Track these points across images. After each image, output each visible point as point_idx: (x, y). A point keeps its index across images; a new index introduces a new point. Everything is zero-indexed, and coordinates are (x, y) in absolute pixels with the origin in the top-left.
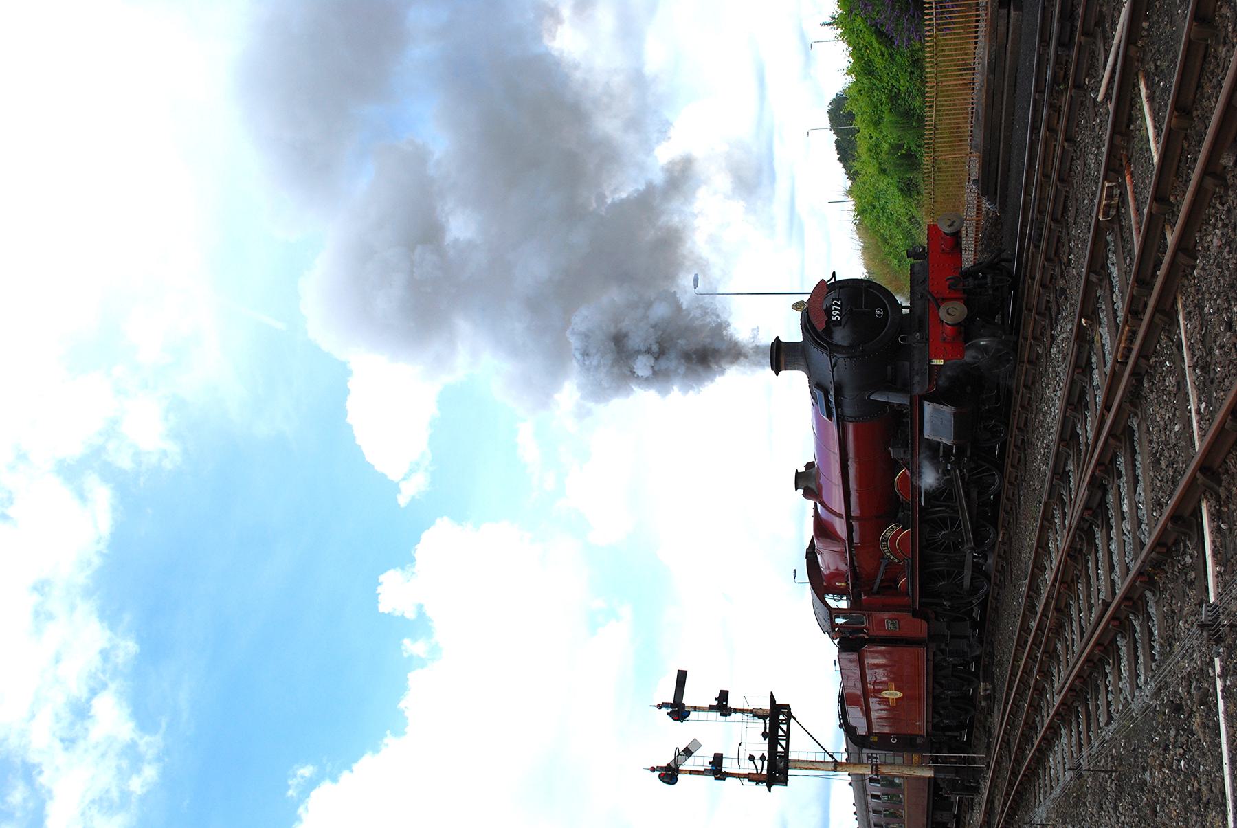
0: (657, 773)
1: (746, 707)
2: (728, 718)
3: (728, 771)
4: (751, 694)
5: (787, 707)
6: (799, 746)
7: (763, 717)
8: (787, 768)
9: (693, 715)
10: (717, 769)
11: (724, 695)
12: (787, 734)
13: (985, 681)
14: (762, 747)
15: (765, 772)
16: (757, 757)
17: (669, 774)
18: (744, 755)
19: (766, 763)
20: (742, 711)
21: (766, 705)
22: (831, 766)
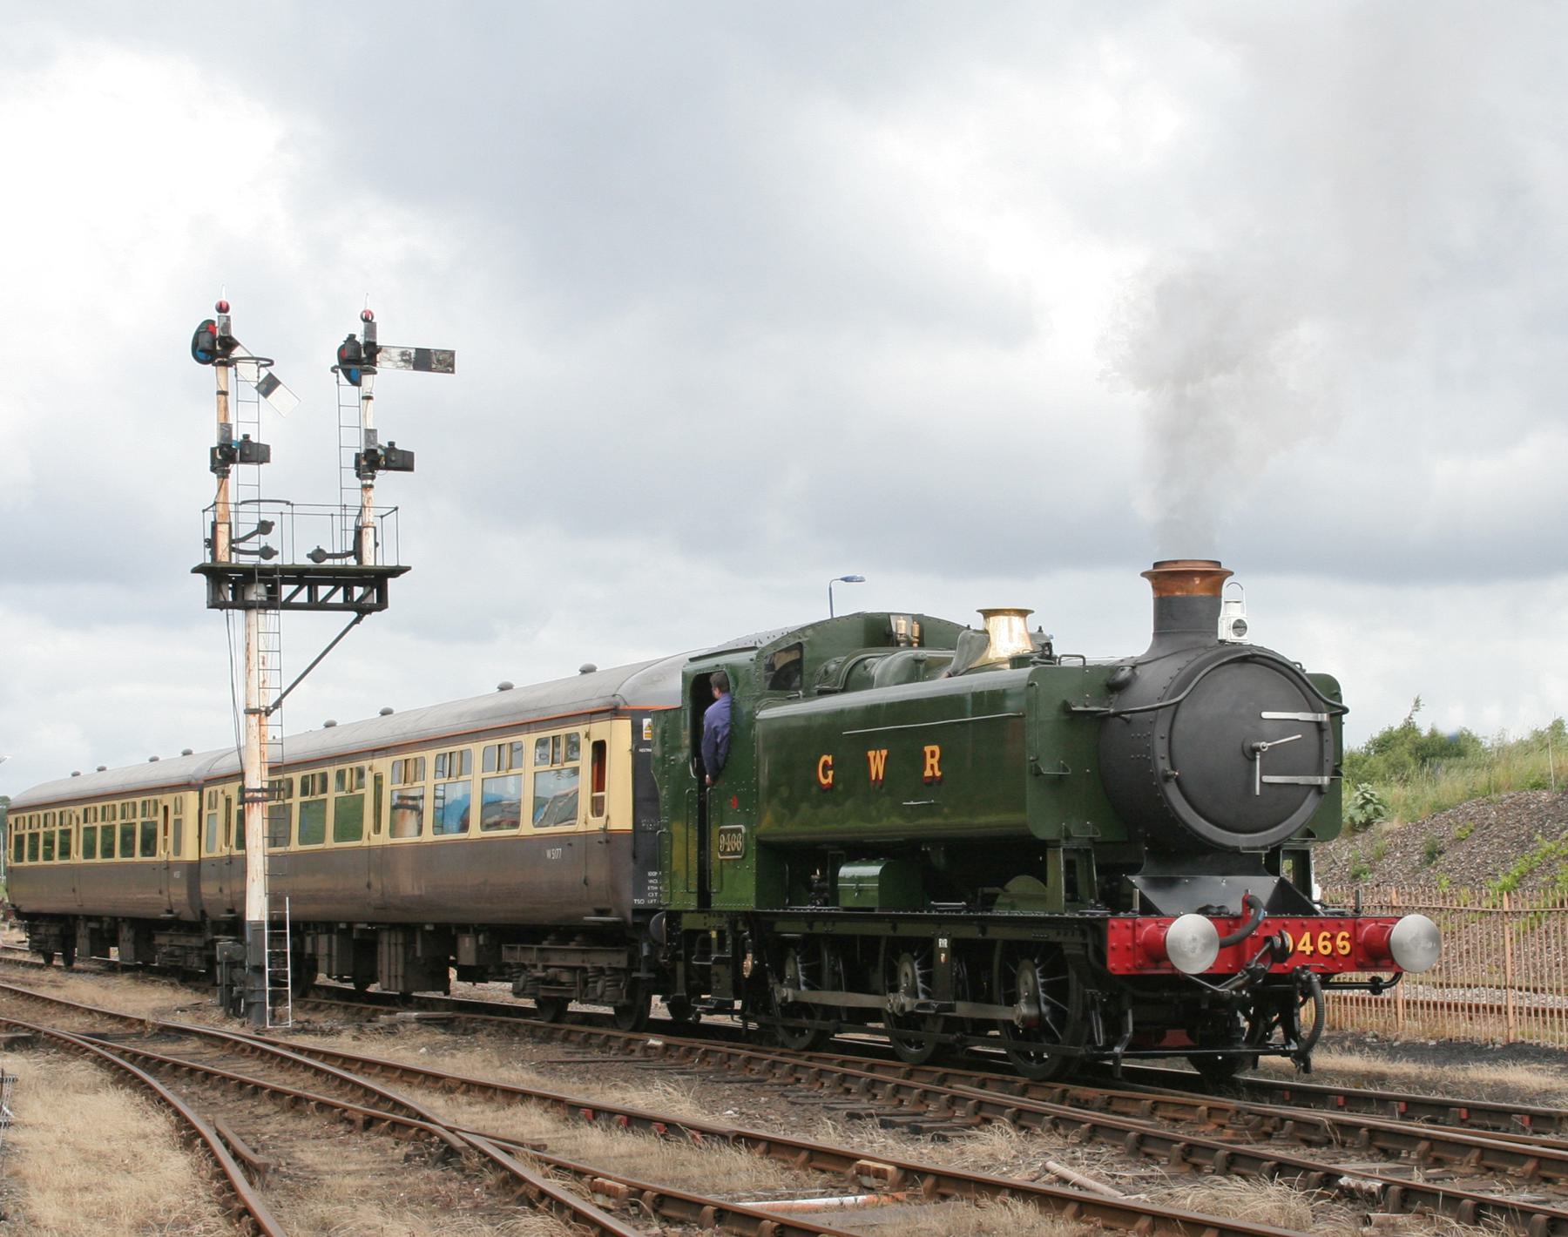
0: (214, 315)
4: (402, 524)
5: (382, 604)
6: (297, 631)
8: (248, 607)
10: (231, 453)
11: (400, 461)
12: (324, 606)
18: (269, 513)
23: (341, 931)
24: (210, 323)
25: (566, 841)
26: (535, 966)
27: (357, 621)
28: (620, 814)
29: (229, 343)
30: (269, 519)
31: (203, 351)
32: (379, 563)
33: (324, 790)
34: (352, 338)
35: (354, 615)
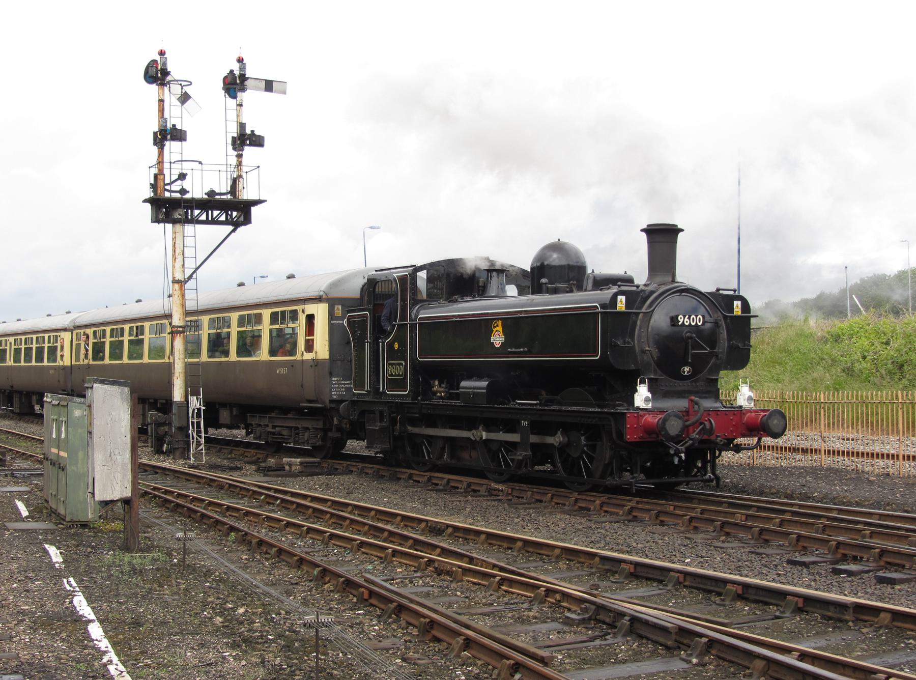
0: (158, 58)
1: (245, 169)
2: (230, 147)
3: (166, 149)
4: (260, 177)
5: (247, 220)
6: (203, 235)
7: (233, 190)
8: (174, 222)
9: (232, 103)
10: (167, 135)
11: (257, 141)
13: (301, 463)
14: (197, 191)
15: (167, 194)
16: (186, 184)
17: (157, 74)
18: (186, 167)
19: (178, 195)
20: (239, 165)
21: (247, 193)
22: (179, 277)
23: (149, 403)
24: (155, 61)
25: (55, 368)
26: (267, 426)
27: (234, 231)
28: (322, 349)
29: (165, 73)
30: (184, 172)
31: (151, 77)
32: (245, 198)
33: (122, 335)
34: (232, 72)
35: (231, 228)
